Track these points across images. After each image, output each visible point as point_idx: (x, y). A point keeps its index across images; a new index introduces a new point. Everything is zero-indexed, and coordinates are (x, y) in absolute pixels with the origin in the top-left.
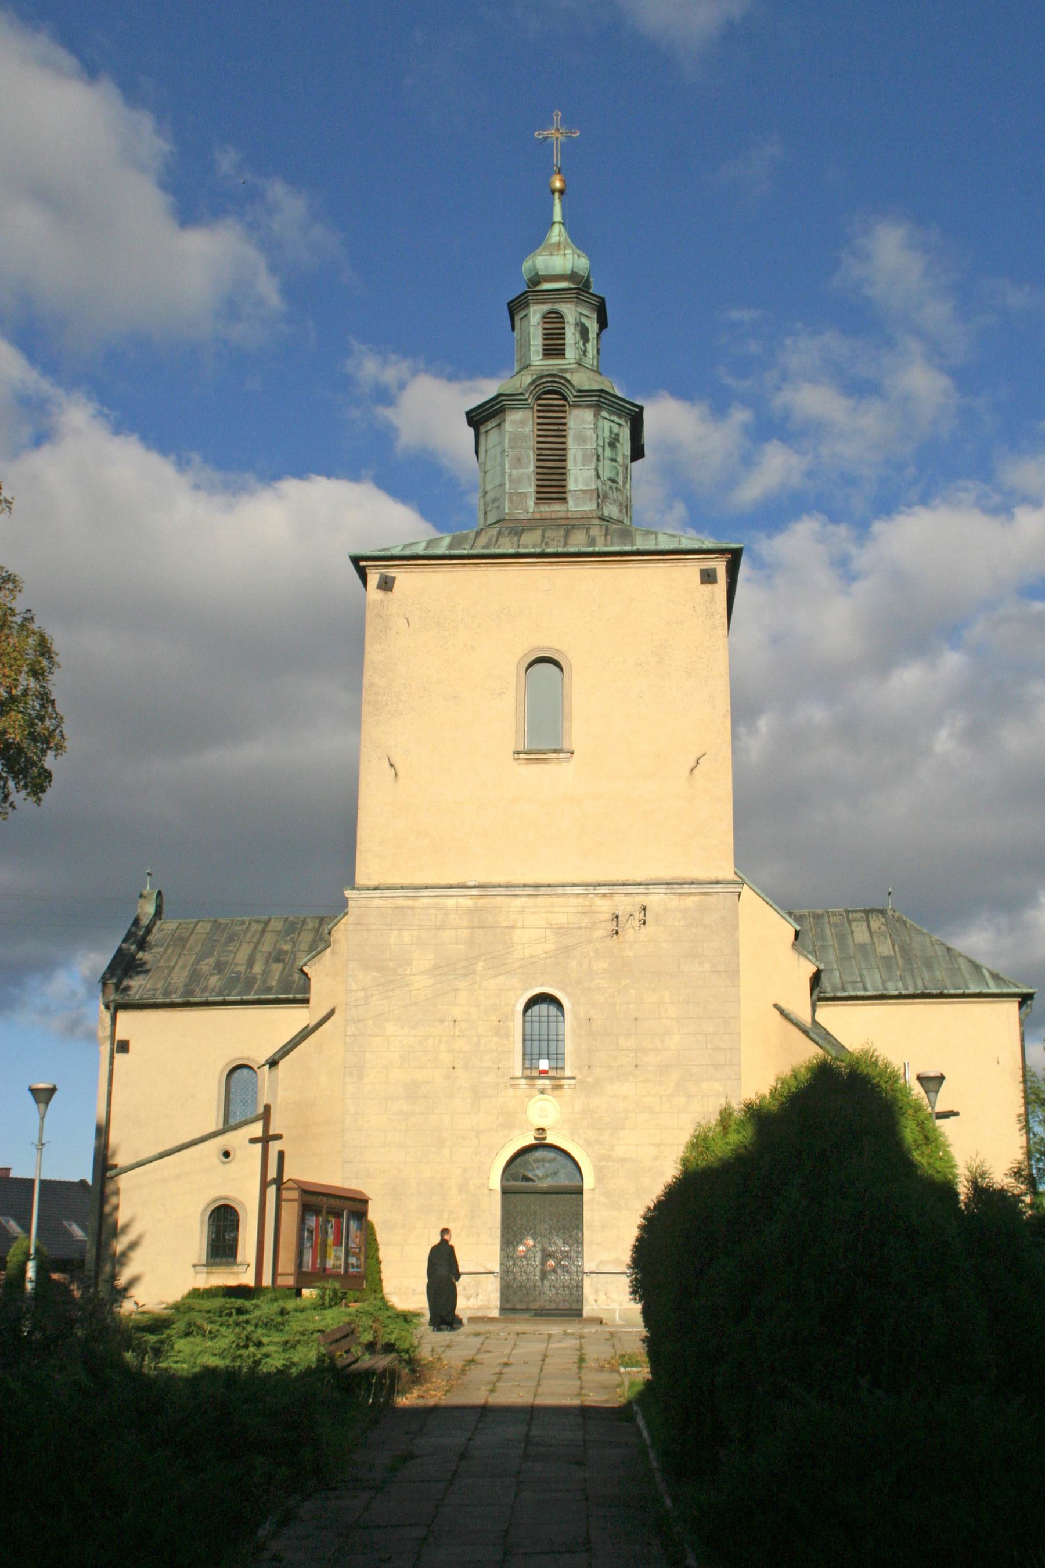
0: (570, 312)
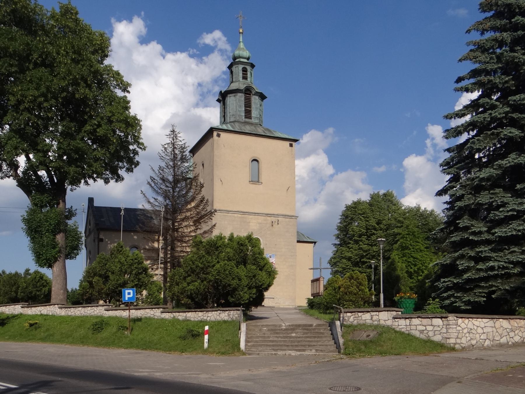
0: (249, 68)
